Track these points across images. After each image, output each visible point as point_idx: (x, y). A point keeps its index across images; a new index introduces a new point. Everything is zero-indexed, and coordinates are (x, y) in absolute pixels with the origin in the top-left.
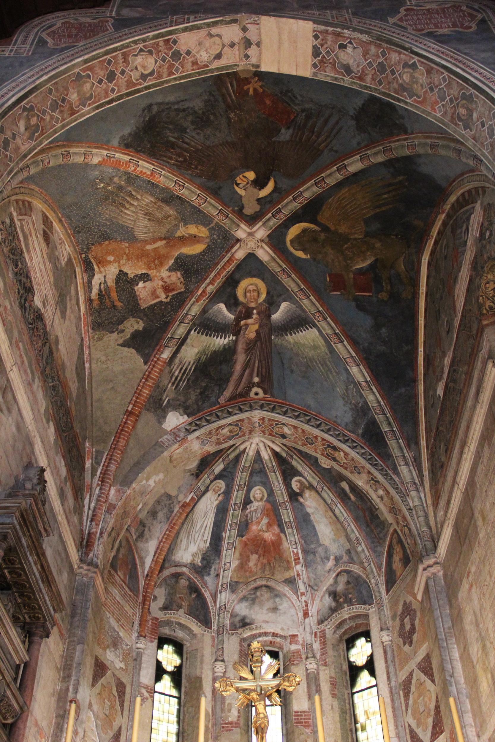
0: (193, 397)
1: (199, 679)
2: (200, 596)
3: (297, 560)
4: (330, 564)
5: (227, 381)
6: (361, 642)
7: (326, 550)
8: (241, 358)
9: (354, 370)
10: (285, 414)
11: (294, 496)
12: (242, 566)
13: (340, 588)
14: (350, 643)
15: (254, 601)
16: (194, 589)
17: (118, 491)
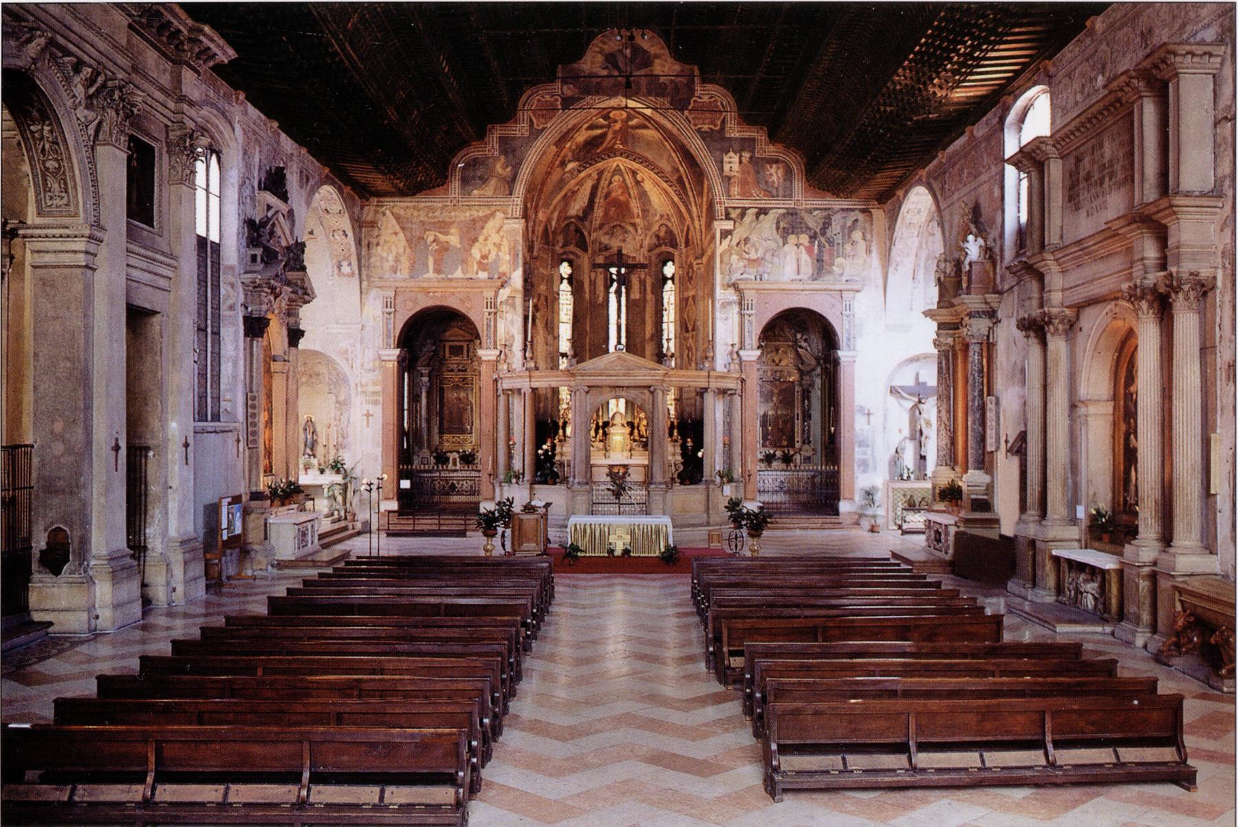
0: (582, 154)
1: (582, 283)
2: (582, 234)
3: (638, 216)
4: (657, 218)
5: (602, 143)
6: (670, 264)
7: (655, 210)
8: (610, 136)
9: (674, 155)
10: (634, 160)
11: (638, 183)
12: (606, 213)
13: (662, 234)
14: (664, 264)
15: (612, 234)
16: (578, 231)
17: (543, 212)
